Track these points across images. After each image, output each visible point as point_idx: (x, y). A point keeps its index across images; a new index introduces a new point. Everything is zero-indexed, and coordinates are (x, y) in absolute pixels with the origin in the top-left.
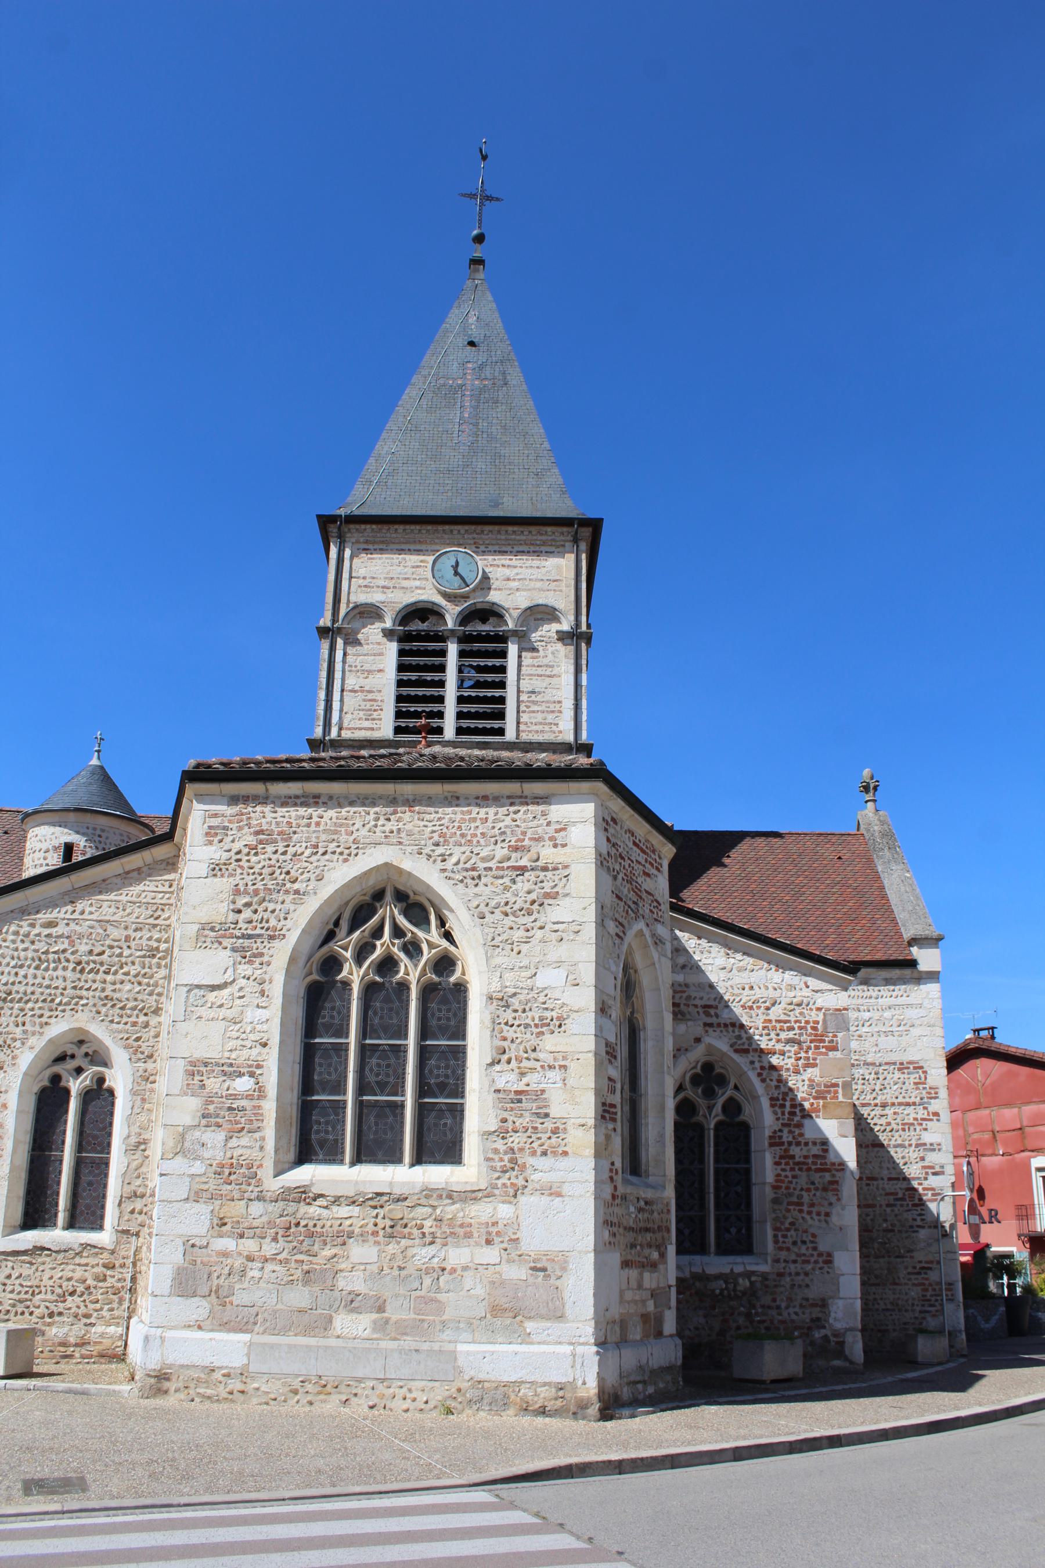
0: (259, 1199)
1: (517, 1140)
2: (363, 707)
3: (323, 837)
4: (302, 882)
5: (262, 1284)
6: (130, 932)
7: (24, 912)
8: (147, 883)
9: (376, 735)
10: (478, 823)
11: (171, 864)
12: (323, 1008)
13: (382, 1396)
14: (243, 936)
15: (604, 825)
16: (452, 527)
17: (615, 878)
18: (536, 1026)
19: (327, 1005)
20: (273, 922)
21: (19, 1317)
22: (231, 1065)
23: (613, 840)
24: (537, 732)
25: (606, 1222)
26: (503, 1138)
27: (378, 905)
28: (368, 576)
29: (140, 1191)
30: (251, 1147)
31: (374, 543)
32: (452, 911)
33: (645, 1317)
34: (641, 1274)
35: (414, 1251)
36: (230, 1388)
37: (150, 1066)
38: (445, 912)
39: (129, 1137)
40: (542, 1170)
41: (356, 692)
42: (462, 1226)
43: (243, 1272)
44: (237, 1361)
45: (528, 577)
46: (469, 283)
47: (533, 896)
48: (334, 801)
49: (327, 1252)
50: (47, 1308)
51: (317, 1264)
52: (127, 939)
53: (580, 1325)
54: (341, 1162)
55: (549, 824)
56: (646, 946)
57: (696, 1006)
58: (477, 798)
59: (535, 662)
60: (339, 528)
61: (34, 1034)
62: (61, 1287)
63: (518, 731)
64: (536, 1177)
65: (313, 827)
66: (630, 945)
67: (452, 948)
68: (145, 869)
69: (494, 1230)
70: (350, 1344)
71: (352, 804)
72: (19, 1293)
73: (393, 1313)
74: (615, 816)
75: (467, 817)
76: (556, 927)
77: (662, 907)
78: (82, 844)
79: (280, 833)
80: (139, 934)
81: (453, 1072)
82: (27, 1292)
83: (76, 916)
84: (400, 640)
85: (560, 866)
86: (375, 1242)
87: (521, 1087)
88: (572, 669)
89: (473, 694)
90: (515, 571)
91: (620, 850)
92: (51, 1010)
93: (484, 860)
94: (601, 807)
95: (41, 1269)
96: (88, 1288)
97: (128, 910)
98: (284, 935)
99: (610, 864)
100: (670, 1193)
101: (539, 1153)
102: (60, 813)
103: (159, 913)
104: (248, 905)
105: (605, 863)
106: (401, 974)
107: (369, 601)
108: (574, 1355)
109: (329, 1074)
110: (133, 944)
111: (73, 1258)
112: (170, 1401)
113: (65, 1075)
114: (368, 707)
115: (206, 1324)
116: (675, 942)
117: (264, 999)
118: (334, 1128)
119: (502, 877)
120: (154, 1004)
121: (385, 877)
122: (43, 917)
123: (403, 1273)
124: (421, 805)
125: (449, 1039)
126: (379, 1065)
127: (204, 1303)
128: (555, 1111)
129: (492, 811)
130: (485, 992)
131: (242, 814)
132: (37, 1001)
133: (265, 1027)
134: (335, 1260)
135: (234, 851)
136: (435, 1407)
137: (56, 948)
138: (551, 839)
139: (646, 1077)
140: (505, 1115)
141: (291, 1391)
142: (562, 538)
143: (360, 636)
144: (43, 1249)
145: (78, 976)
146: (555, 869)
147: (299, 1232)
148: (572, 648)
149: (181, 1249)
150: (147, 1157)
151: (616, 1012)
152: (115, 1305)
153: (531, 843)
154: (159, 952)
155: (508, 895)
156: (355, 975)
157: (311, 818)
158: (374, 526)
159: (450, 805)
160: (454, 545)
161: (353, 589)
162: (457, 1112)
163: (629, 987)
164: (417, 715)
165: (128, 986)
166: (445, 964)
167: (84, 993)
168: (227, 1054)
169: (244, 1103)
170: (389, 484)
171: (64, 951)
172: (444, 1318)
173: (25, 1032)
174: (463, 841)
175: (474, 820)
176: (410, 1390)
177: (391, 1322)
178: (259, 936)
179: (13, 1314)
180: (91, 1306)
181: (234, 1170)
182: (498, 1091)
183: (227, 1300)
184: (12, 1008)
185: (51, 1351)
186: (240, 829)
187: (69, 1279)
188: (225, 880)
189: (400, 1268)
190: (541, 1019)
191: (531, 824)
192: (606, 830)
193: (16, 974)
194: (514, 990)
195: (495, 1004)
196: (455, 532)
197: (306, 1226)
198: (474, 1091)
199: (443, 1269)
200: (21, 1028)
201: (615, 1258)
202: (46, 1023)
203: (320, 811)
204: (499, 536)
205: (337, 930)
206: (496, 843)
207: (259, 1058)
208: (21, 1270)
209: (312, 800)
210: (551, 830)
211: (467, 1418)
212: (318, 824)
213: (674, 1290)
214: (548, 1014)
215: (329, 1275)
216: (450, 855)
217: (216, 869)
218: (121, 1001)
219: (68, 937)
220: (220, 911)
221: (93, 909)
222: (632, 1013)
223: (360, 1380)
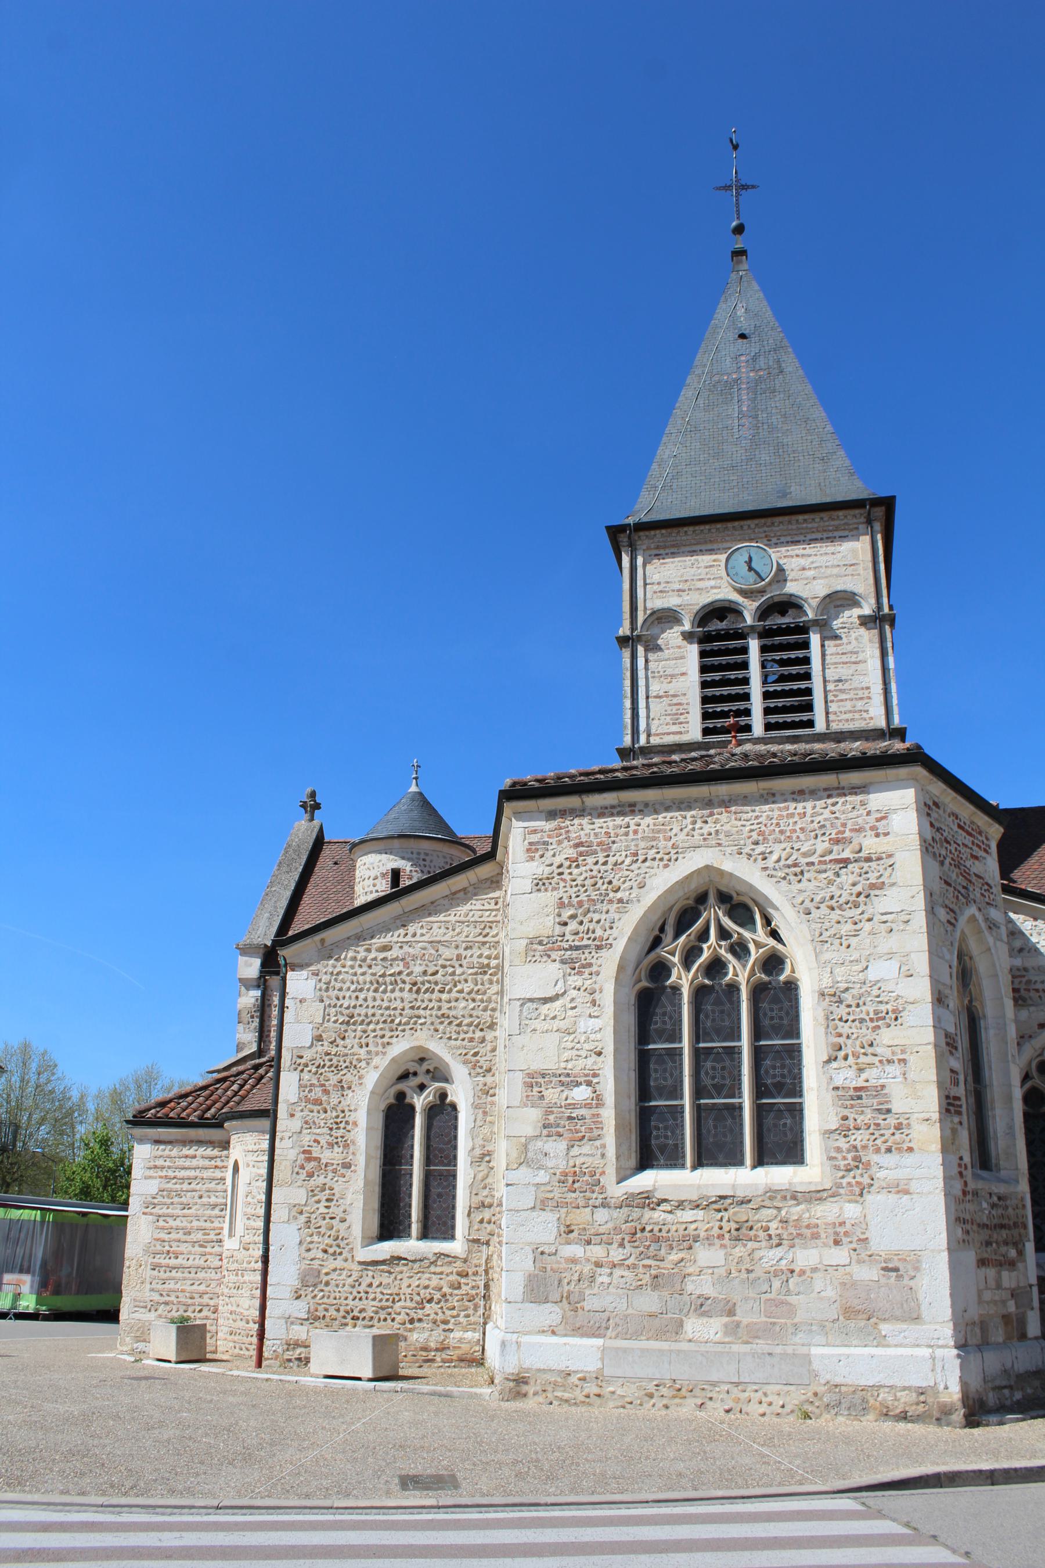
0: (604, 1205)
1: (859, 1138)
3: (642, 844)
4: (624, 890)
5: (612, 1289)
6: (461, 951)
7: (359, 938)
8: (474, 902)
9: (685, 738)
10: (796, 818)
11: (495, 882)
12: (654, 1014)
13: (737, 1400)
14: (571, 948)
15: (927, 809)
16: (742, 523)
17: (942, 863)
18: (871, 1020)
19: (658, 1011)
20: (599, 932)
21: (382, 1323)
22: (568, 1075)
23: (937, 825)
24: (847, 720)
25: (958, 1219)
26: (845, 1136)
27: (702, 908)
28: (662, 581)
29: (487, 1201)
30: (592, 1155)
31: (665, 547)
32: (777, 909)
33: (1006, 1318)
34: (999, 1273)
35: (761, 1253)
36: (586, 1391)
37: (489, 1079)
38: (770, 910)
39: (473, 1149)
40: (888, 1167)
41: (660, 697)
42: (808, 1227)
43: (592, 1278)
44: (591, 1365)
45: (824, 565)
46: (733, 276)
47: (858, 888)
48: (650, 808)
49: (674, 1257)
50: (408, 1314)
51: (664, 1268)
52: (459, 957)
53: (937, 1327)
54: (683, 1166)
55: (869, 813)
56: (980, 931)
57: (1037, 990)
58: (793, 793)
59: (839, 650)
60: (629, 537)
61: (377, 1054)
62: (419, 1294)
63: (828, 721)
64: (882, 1174)
65: (631, 836)
66: (963, 932)
67: (780, 947)
68: (471, 889)
69: (842, 1230)
70: (703, 1348)
71: (668, 809)
72: (381, 1300)
73: (744, 1317)
74: (936, 800)
75: (785, 813)
76: (885, 918)
77: (994, 890)
78: (408, 868)
79: (599, 844)
80: (469, 953)
81: (790, 1071)
82: (387, 1300)
83: (409, 938)
84: (700, 642)
85: (884, 855)
86: (721, 1245)
87: (860, 1083)
88: (877, 653)
89: (779, 689)
90: (811, 559)
91: (945, 834)
92: (392, 1031)
93: (805, 855)
94: (921, 791)
95: (399, 1277)
96: (444, 1296)
97: (458, 930)
98: (611, 945)
99: (935, 850)
100: (1024, 1187)
101: (883, 1150)
103: (487, 930)
104: (573, 917)
105: (930, 849)
106: (730, 975)
107: (666, 606)
108: (933, 1358)
109: (665, 1079)
110: (464, 962)
111: (428, 1267)
112: (530, 1404)
113: (409, 1092)
114: (674, 711)
115: (560, 1329)
116: (1010, 925)
117: (596, 1008)
118: (673, 1133)
119: (825, 871)
120: (489, 1019)
121: (707, 879)
122: (378, 941)
123: (752, 1276)
124: (737, 805)
125: (783, 1038)
126: (714, 1068)
127: (556, 1308)
128: (896, 1106)
129: (809, 805)
130: (817, 988)
131: (561, 828)
132: (378, 1023)
133: (599, 1036)
134: (682, 1264)
135: (556, 865)
136: (792, 1412)
137: (392, 971)
138: (872, 828)
139: (990, 1068)
140: (846, 1112)
141: (646, 1395)
142: (855, 521)
143: (660, 642)
144: (400, 1258)
145: (415, 996)
146: (879, 859)
147: (644, 1236)
148: (876, 632)
149: (531, 1257)
150: (492, 1168)
151: (953, 1002)
152: (471, 1312)
153: (853, 834)
154: (490, 968)
155: (833, 888)
156: (684, 980)
157: (628, 827)
158: (664, 531)
159: (766, 802)
160: (746, 541)
161: (648, 595)
162: (797, 1112)
163: (965, 975)
164: (724, 715)
165: (463, 1004)
166: (773, 962)
167: (422, 1012)
168: (563, 1065)
169: (583, 1112)
170: (674, 487)
171: (400, 973)
172: (796, 1320)
173: (369, 1053)
174: (782, 838)
175: (792, 815)
176: (765, 1394)
177: (742, 1326)
178: (587, 946)
179: (376, 1320)
180: (448, 1313)
181: (577, 1178)
182: (837, 1088)
183: (578, 1305)
184: (355, 1031)
185: (414, 1356)
186: (560, 843)
187: (426, 1287)
188: (549, 894)
189: (749, 1271)
190: (876, 1012)
191: (850, 815)
192: (928, 815)
193: (357, 997)
194: (846, 985)
195: (827, 1000)
196: (745, 527)
197: (651, 1231)
198: (812, 1089)
199: (792, 1271)
200: (365, 1049)
201: (970, 1257)
202: (388, 1043)
203: (637, 819)
204: (790, 527)
205: (663, 936)
206: (816, 837)
207: (595, 1067)
208: (381, 1279)
209: (628, 809)
210: (871, 819)
211: (824, 1422)
212: (636, 832)
213: (1035, 1290)
214: (883, 1008)
215: (678, 1279)
216: (771, 852)
217: (540, 884)
218: (457, 1018)
219: (402, 960)
220: (546, 925)
221: (424, 931)
222: (970, 1001)
223: (714, 1384)
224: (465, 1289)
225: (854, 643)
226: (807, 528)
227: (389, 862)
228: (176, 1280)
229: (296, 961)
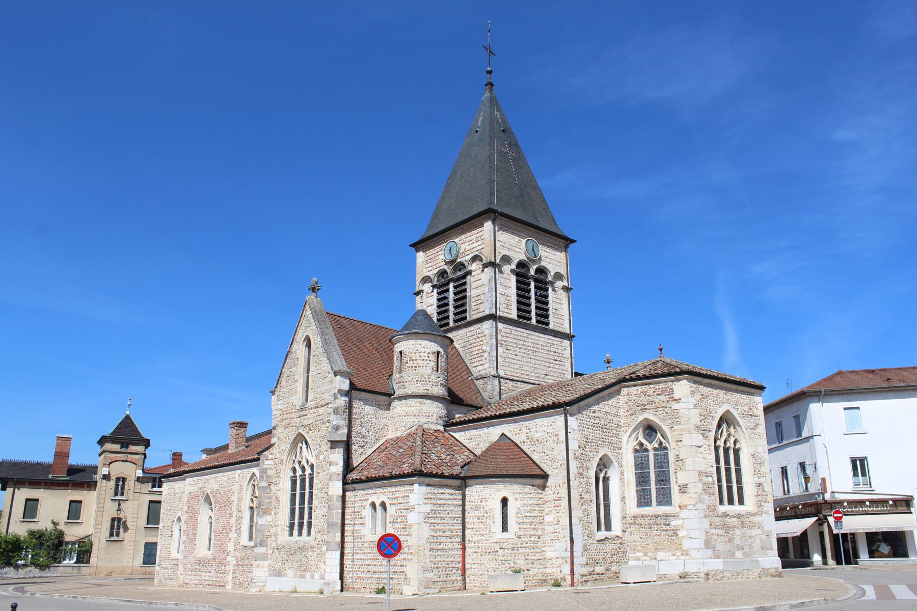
1: (760, 498)
9: (511, 316)
44: (721, 567)
122: (593, 408)
224: (622, 550)
227: (435, 347)
228: (441, 556)
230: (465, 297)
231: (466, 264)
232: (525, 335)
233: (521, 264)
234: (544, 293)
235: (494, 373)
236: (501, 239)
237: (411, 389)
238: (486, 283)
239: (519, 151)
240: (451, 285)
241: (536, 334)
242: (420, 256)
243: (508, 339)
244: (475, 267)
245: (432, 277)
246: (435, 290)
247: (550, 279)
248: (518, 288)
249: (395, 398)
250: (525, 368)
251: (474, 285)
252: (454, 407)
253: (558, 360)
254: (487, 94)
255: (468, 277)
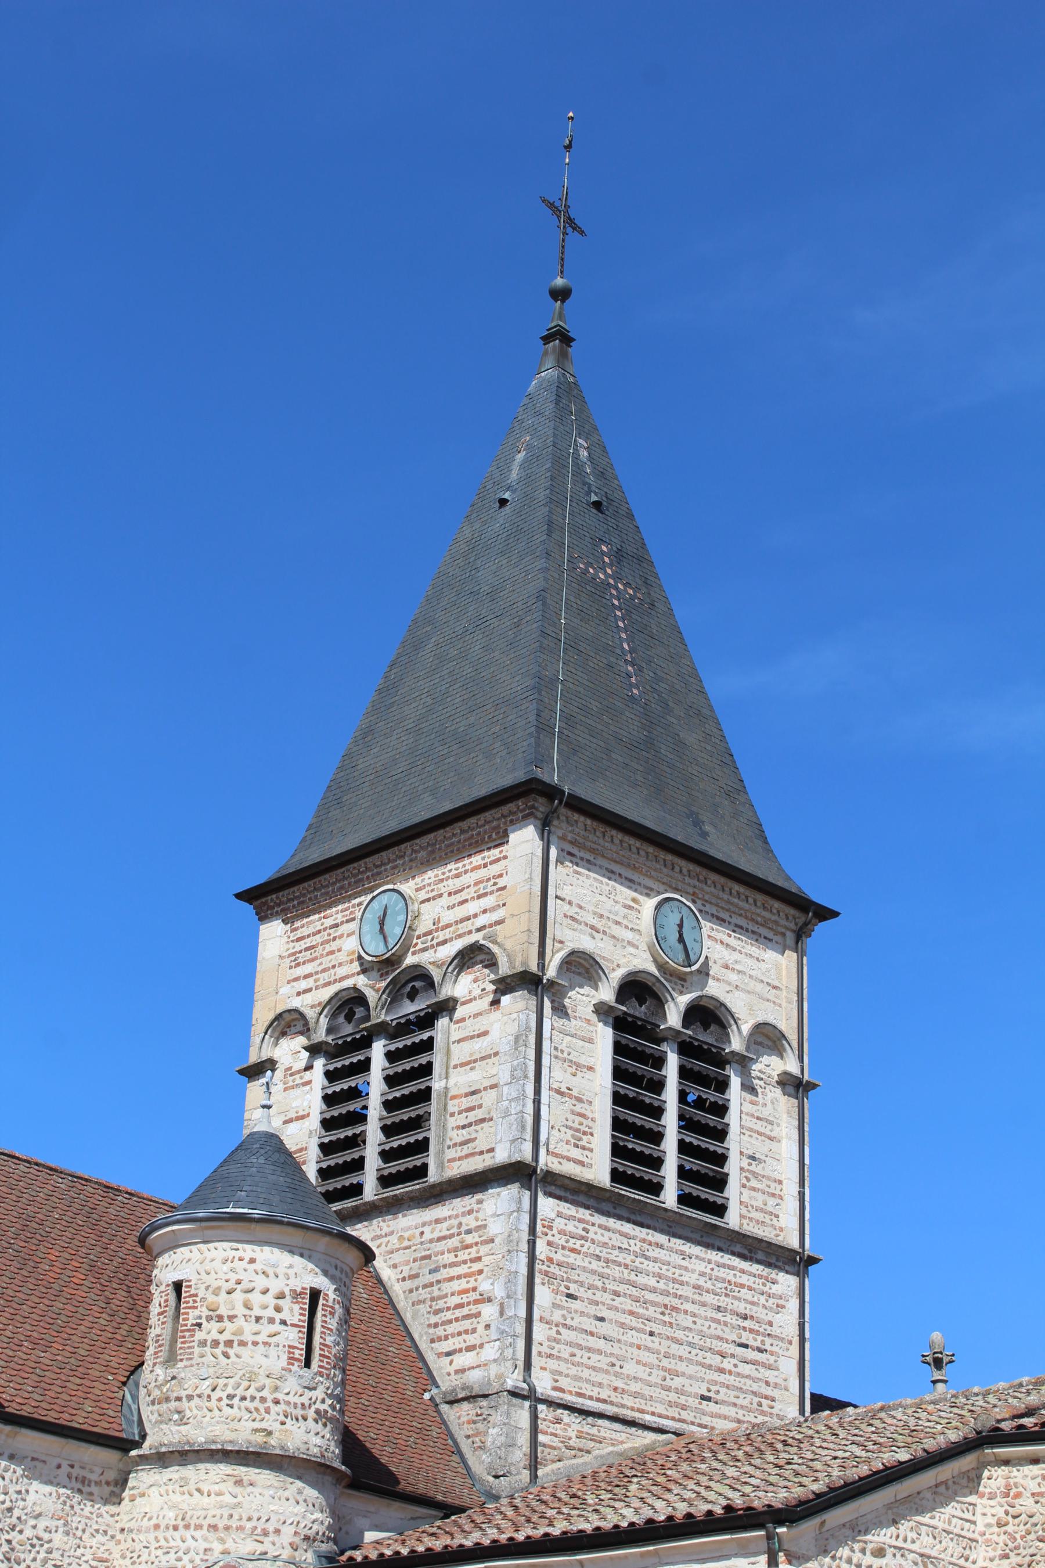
2: (570, 1123)
9: (587, 1175)
24: (758, 1222)
28: (575, 901)
31: (581, 847)
41: (562, 1094)
68: (950, 1483)
90: (736, 956)
102: (310, 1233)
103: (967, 1552)
114: (576, 1125)
142: (783, 922)
143: (567, 1002)
158: (589, 822)
196: (677, 869)
225: (769, 1105)
226: (736, 906)
229: (793, 1549)
230: (425, 1095)
231: (436, 975)
232: (636, 1246)
233: (635, 988)
234: (711, 1096)
235: (514, 1380)
236: (566, 892)
237: (206, 1427)
238: (505, 1046)
239: (648, 580)
240: (378, 1050)
241: (677, 1243)
242: (274, 937)
243: (572, 1258)
244: (466, 986)
245: (310, 1014)
246: (319, 1064)
247: (736, 1044)
248: (619, 1073)
249: (143, 1459)
250: (630, 1368)
251: (460, 1053)
252: (359, 1502)
253: (754, 1346)
254: (549, 373)
255: (442, 1023)
